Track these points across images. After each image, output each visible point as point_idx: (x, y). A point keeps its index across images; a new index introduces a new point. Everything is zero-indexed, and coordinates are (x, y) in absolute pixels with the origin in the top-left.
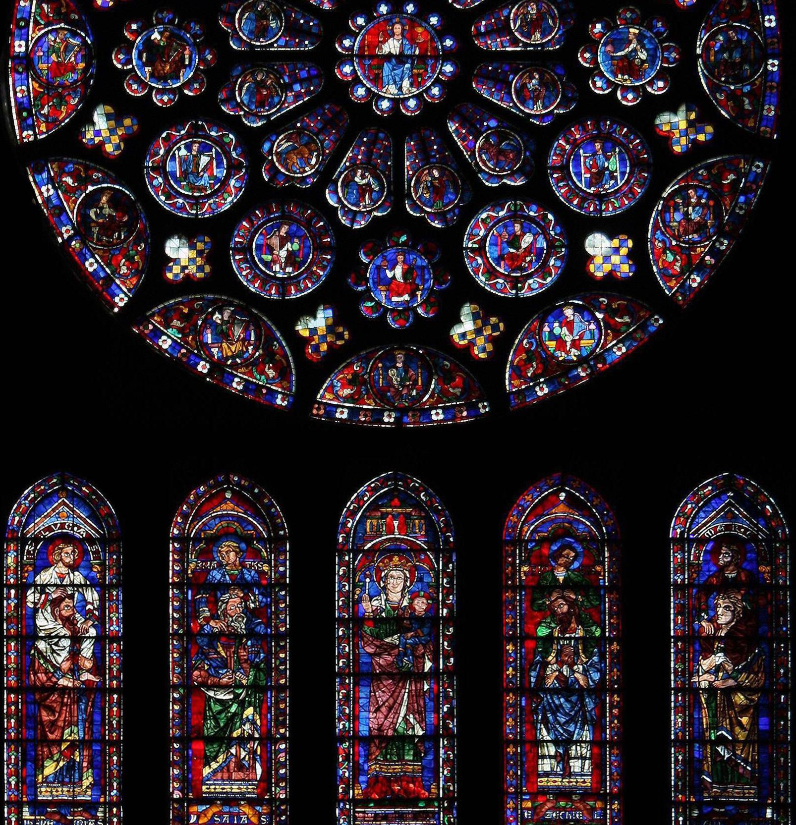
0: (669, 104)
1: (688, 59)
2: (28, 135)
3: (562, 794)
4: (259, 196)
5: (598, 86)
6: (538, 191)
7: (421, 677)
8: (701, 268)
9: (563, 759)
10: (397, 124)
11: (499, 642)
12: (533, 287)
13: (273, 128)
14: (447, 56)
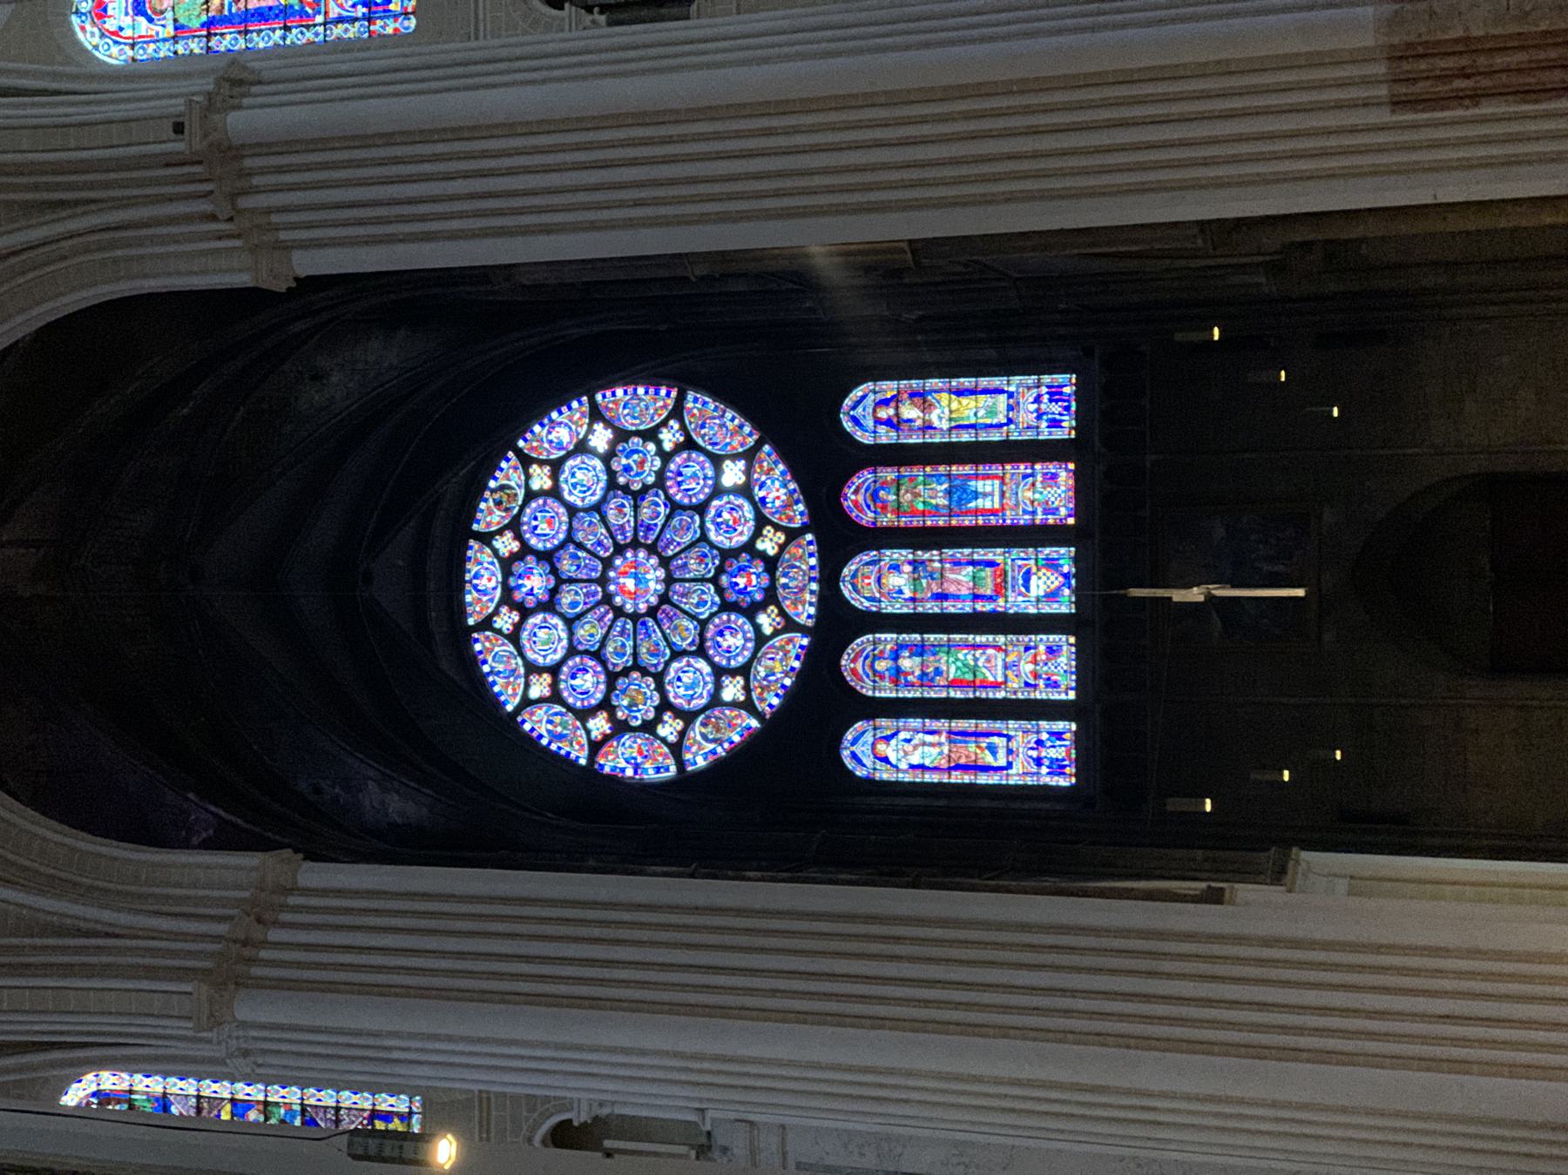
0: (659, 443)
1: (638, 433)
2: (673, 769)
3: (1003, 494)
4: (701, 652)
5: (651, 480)
6: (701, 509)
7: (943, 568)
8: (741, 427)
9: (985, 495)
10: (669, 580)
11: (924, 530)
12: (748, 512)
13: (670, 644)
14: (635, 556)
